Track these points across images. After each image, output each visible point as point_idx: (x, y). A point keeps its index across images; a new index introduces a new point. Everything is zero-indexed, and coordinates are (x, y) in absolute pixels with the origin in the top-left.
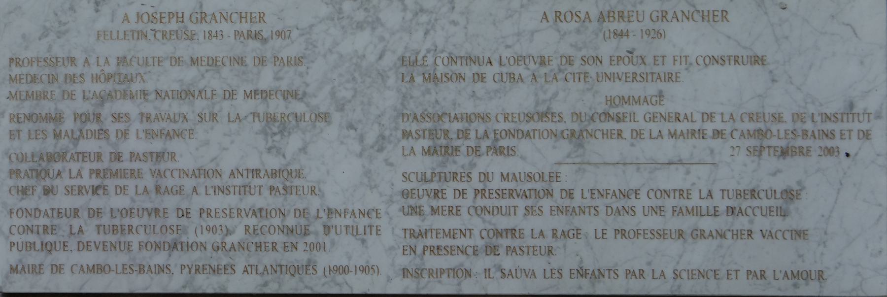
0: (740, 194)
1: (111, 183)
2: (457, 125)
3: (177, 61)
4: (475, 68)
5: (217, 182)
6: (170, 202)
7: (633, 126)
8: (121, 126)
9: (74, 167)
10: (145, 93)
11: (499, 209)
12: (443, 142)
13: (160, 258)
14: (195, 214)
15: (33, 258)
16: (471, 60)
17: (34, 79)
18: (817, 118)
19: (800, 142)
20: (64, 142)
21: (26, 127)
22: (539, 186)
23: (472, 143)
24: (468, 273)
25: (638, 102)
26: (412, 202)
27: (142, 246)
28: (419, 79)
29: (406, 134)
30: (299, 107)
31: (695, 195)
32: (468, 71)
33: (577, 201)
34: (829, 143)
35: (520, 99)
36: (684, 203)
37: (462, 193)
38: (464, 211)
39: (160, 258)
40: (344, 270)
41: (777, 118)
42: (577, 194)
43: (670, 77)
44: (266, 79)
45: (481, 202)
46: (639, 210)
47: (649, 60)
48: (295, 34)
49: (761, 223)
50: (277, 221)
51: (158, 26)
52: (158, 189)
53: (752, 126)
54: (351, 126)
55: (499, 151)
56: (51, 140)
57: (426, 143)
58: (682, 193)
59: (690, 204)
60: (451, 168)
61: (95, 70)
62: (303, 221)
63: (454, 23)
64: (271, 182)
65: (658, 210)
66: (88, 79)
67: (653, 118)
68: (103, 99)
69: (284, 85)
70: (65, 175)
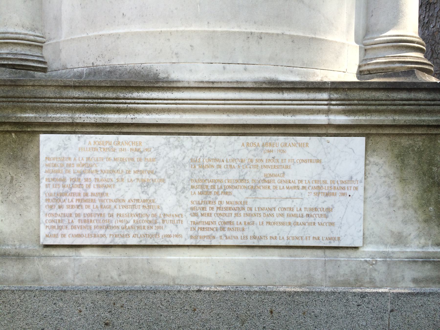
0: (311, 209)
1: (84, 204)
2: (211, 184)
3: (110, 159)
4: (218, 163)
5: (123, 204)
6: (106, 211)
7: (274, 184)
8: (88, 183)
9: (70, 198)
10: (97, 171)
11: (226, 214)
12: (206, 190)
13: (102, 232)
14: (115, 216)
15: (55, 232)
16: (216, 160)
17: (55, 165)
18: (339, 182)
19: (333, 191)
20: (66, 189)
21: (52, 183)
22: (240, 206)
23: (216, 190)
24: (214, 237)
25: (276, 176)
26: (194, 212)
27: (96, 227)
28: (197, 167)
29: (193, 187)
30: (154, 177)
31: (295, 210)
32: (215, 164)
33: (253, 212)
34: (343, 191)
35: (233, 174)
36: (291, 212)
37: (212, 208)
38: (213, 215)
39: (102, 232)
40: (169, 236)
41: (325, 182)
42: (253, 209)
43: (287, 167)
44: (142, 166)
45: (219, 212)
46: (275, 215)
47: (280, 161)
48: (152, 150)
49: (318, 220)
50: (145, 218)
51: (102, 146)
52: (101, 206)
53: (316, 185)
54: (172, 184)
55: (226, 193)
56: (61, 188)
57: (200, 190)
58: (291, 209)
59: (293, 213)
60: (209, 199)
61: (78, 162)
62: (155, 218)
63: (210, 146)
64: (143, 204)
65: (282, 215)
66: (75, 165)
67: (281, 182)
68: (81, 173)
69: (148, 168)
70: (67, 201)
